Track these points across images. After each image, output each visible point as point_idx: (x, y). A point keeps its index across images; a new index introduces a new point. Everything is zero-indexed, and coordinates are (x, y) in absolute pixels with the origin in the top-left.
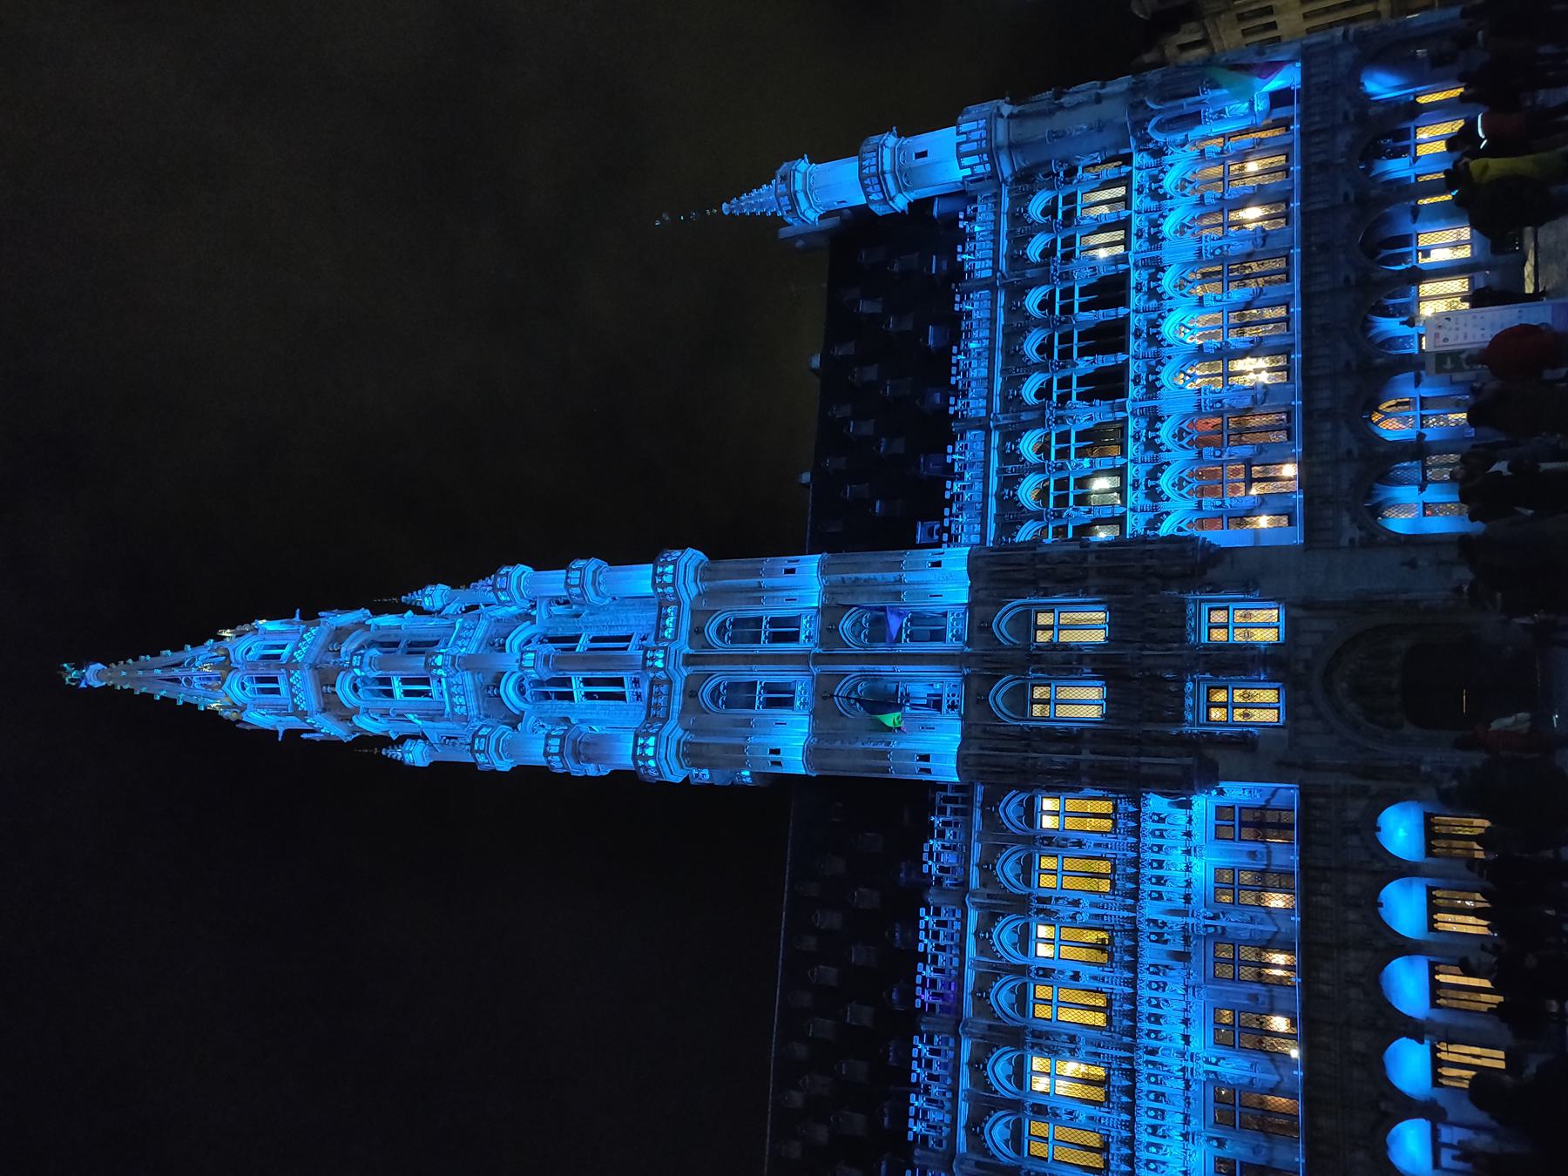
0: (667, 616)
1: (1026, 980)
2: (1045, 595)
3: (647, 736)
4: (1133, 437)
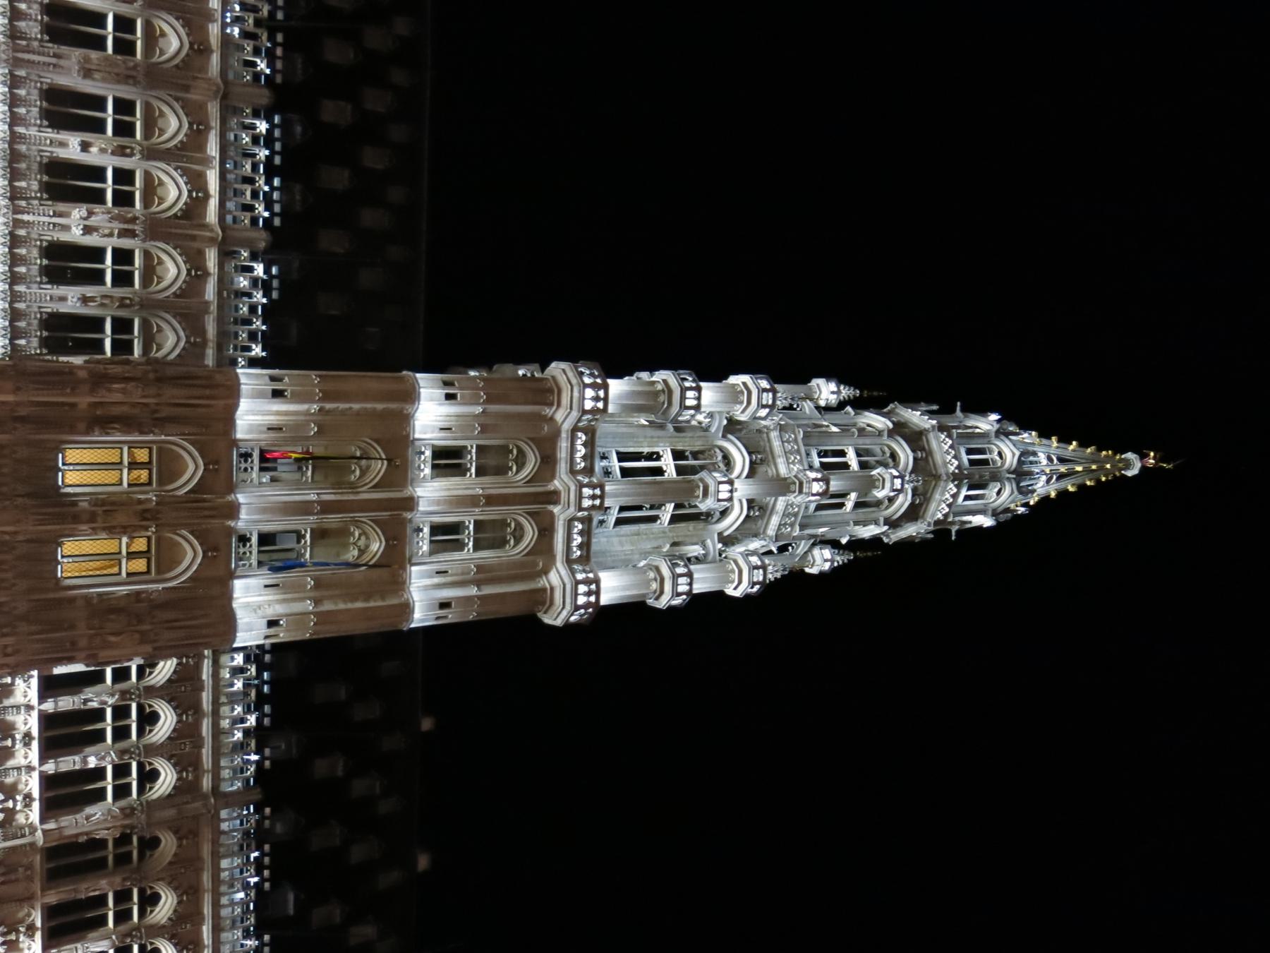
0: (580, 547)
1: (145, 143)
2: (138, 593)
3: (594, 411)
4: (32, 800)
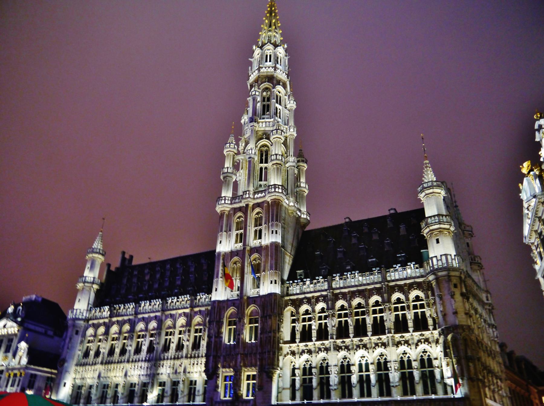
0: (261, 193)
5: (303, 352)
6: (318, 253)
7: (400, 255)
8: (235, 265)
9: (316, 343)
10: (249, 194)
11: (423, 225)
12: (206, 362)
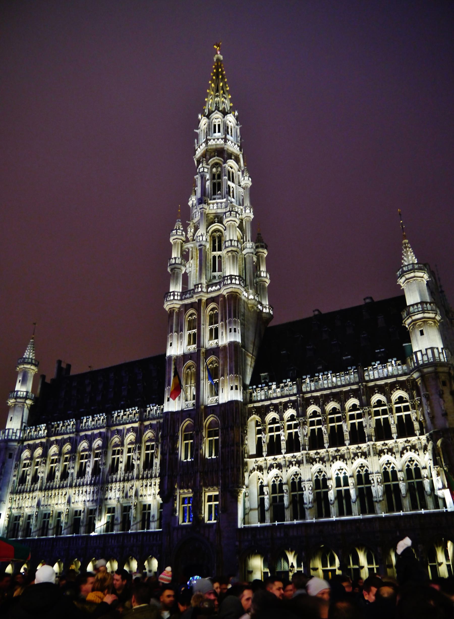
0: (216, 286)
5: (271, 466)
6: (284, 352)
7: (379, 351)
8: (188, 370)
9: (286, 455)
10: (201, 287)
11: (405, 314)
12: (160, 482)
